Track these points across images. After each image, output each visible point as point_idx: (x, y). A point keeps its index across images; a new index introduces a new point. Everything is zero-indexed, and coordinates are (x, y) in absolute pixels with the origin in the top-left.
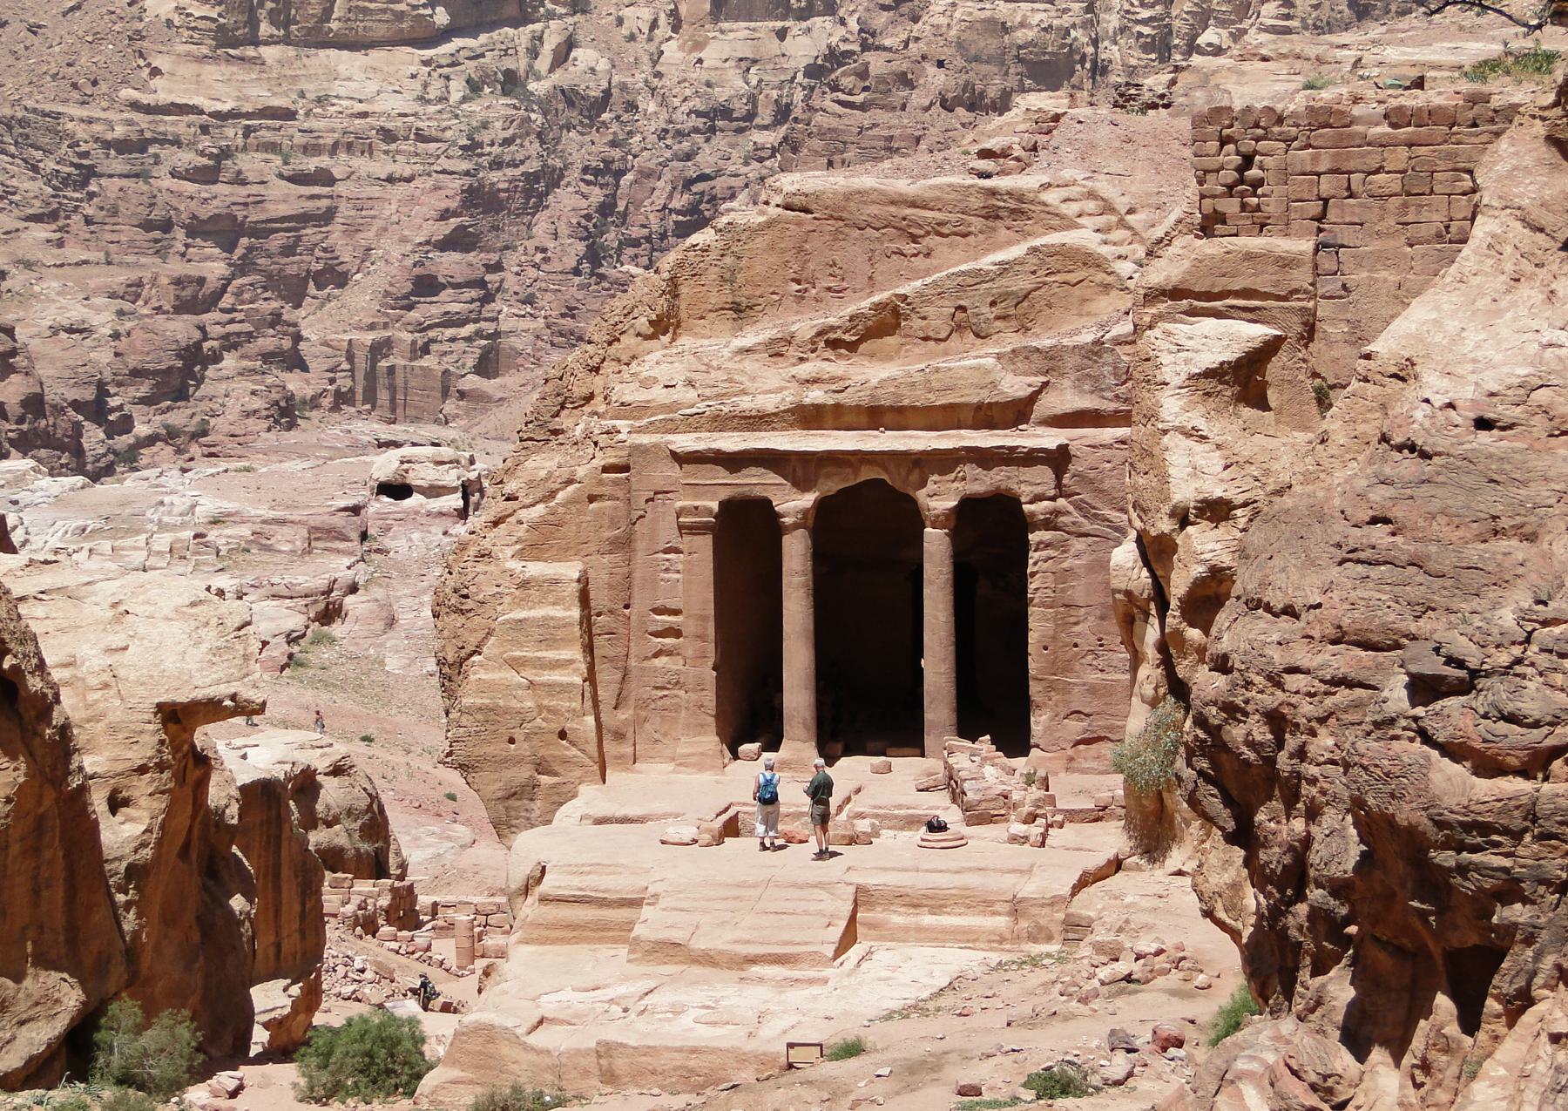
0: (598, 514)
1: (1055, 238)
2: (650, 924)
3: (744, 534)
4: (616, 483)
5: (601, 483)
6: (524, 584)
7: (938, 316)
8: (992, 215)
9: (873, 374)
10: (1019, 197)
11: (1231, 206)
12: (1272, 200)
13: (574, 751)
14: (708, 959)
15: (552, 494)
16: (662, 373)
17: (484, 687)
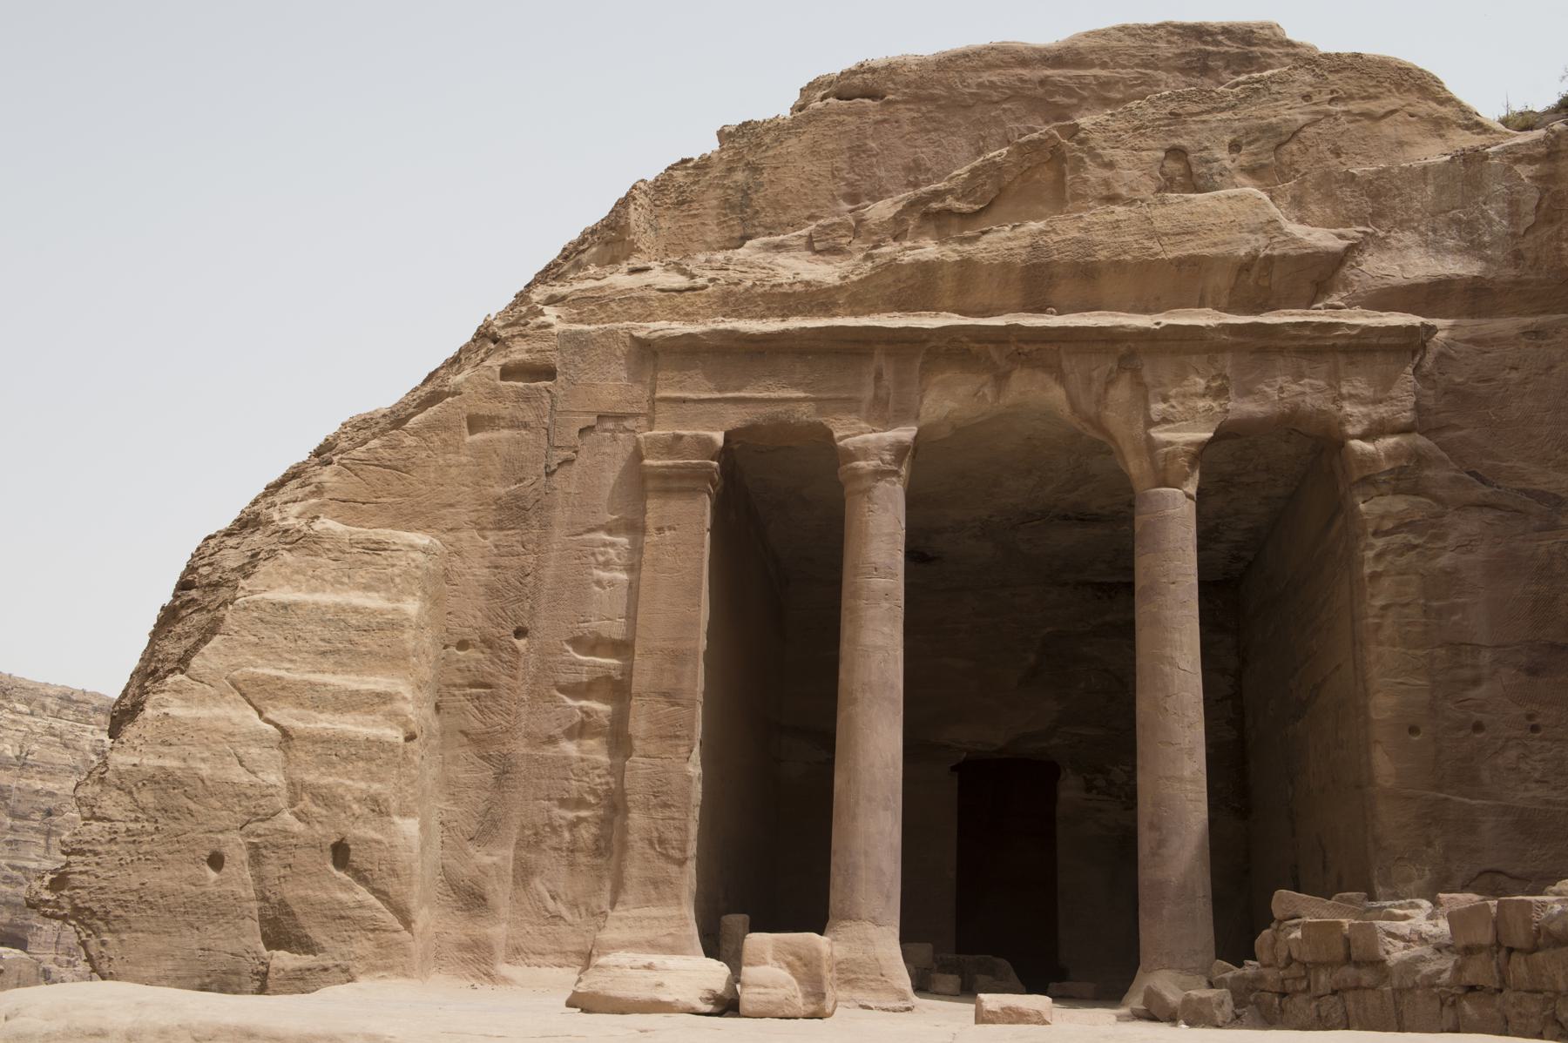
0: (480, 452)
4: (525, 398)
5: (495, 394)
13: (363, 894)
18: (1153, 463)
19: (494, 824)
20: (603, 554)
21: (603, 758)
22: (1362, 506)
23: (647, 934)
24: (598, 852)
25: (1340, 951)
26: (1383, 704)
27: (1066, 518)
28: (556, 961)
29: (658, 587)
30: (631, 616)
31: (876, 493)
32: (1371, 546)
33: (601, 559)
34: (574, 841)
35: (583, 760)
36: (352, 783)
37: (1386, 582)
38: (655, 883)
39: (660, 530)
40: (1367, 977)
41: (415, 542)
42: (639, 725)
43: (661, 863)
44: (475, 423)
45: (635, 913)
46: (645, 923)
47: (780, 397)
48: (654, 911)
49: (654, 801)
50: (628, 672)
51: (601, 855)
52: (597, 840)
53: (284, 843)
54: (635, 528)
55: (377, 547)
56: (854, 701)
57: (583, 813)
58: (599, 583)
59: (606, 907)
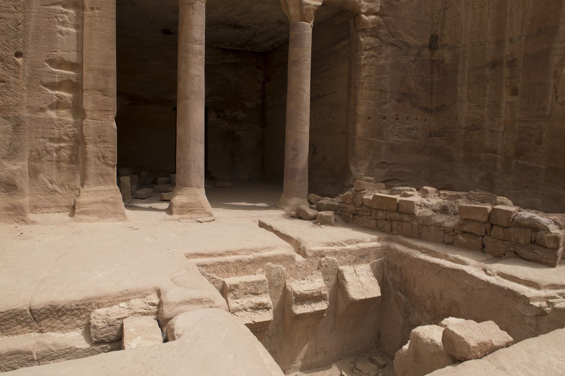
18: (301, 11)
19: (15, 150)
20: (62, 17)
21: (70, 119)
22: (362, 39)
23: (101, 198)
24: (71, 162)
25: (395, 208)
26: (362, 109)
27: (230, 25)
28: (57, 210)
30: (80, 50)
31: (196, 6)
32: (363, 54)
33: (61, 20)
34: (59, 157)
35: (60, 120)
37: (366, 68)
38: (102, 176)
39: (92, 9)
40: (406, 218)
42: (88, 104)
43: (104, 167)
45: (94, 188)
46: (100, 193)
48: (103, 188)
49: (98, 139)
50: (81, 78)
51: (73, 163)
52: (70, 156)
56: (187, 98)
57: (62, 145)
58: (61, 32)
59: (78, 186)
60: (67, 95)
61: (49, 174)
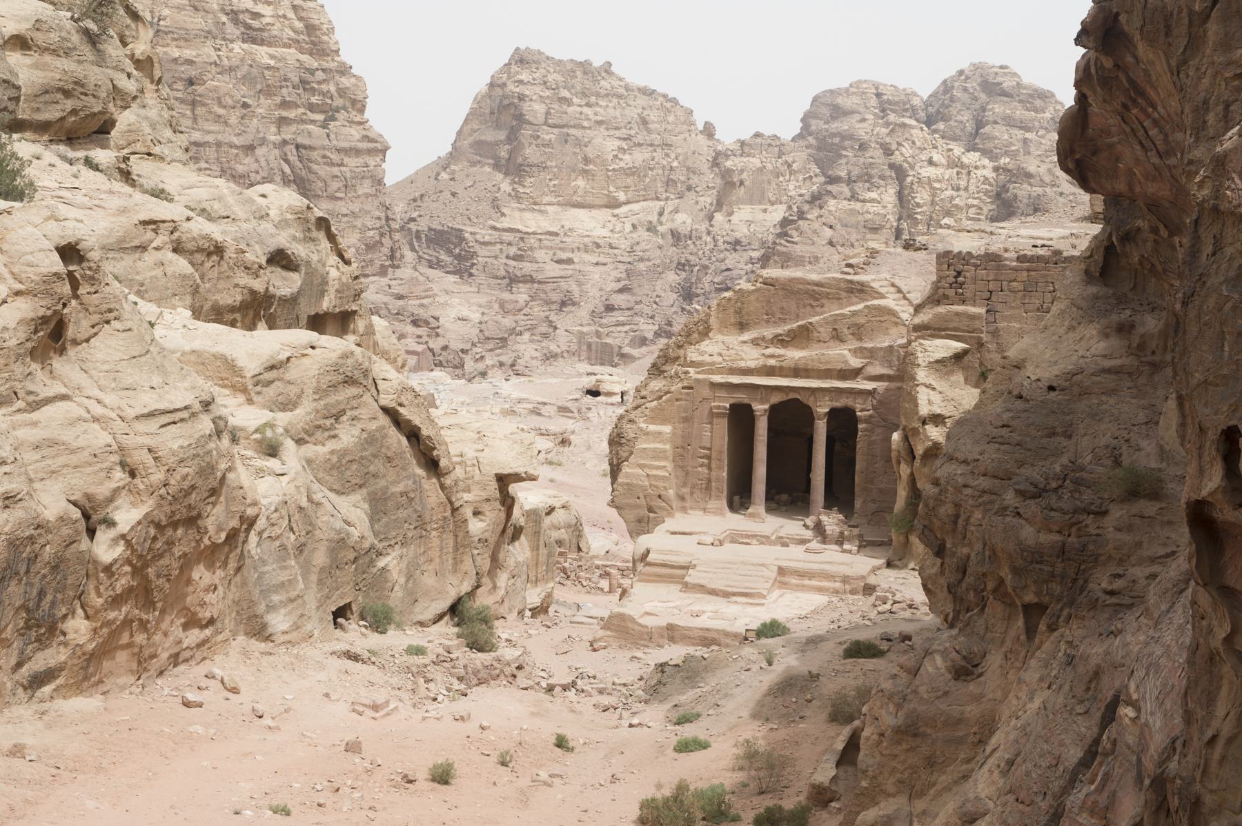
0: (679, 407)
1: (876, 302)
2: (693, 577)
3: (741, 418)
4: (687, 394)
6: (647, 434)
7: (825, 332)
8: (851, 291)
9: (795, 355)
10: (862, 284)
11: (951, 292)
12: (968, 291)
14: (714, 592)
15: (661, 397)
16: (710, 349)
17: (628, 475)
29: (718, 436)
36: (661, 484)
41: (667, 429)
42: (713, 466)
44: (677, 400)
47: (742, 397)
53: (650, 495)
54: (711, 423)
55: (660, 433)
60: (705, 461)
61: (698, 494)
